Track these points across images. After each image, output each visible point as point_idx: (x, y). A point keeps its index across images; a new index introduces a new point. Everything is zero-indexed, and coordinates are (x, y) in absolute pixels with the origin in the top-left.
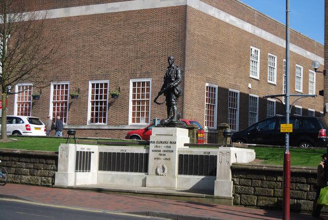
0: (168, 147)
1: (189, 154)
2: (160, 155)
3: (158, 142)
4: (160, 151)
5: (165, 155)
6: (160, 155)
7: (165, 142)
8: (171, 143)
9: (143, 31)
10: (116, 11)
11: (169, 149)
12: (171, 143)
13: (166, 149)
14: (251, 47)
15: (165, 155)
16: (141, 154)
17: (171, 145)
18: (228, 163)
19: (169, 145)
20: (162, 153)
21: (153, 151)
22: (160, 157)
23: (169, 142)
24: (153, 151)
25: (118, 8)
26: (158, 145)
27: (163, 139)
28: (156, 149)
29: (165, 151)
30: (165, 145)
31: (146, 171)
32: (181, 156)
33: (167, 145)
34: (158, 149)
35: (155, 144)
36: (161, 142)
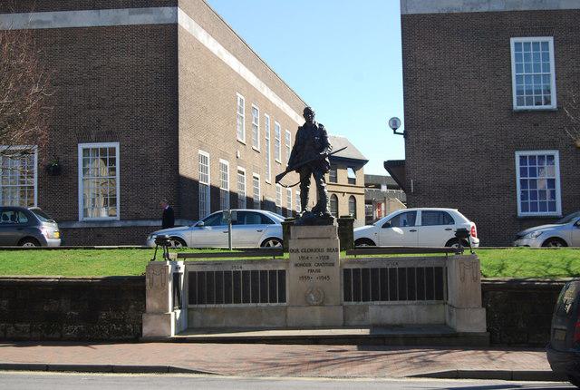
1: (361, 267)
2: (312, 271)
3: (304, 251)
5: (319, 271)
6: (312, 271)
8: (329, 250)
9: (98, 63)
10: (46, 27)
12: (329, 250)
14: (238, 94)
16: (273, 273)
17: (328, 254)
18: (476, 279)
20: (315, 268)
21: (296, 265)
22: (310, 274)
24: (296, 265)
25: (49, 22)
26: (304, 254)
27: (314, 244)
28: (300, 262)
30: (316, 254)
31: (283, 299)
32: (346, 272)
33: (321, 254)
34: (307, 261)
36: (311, 250)
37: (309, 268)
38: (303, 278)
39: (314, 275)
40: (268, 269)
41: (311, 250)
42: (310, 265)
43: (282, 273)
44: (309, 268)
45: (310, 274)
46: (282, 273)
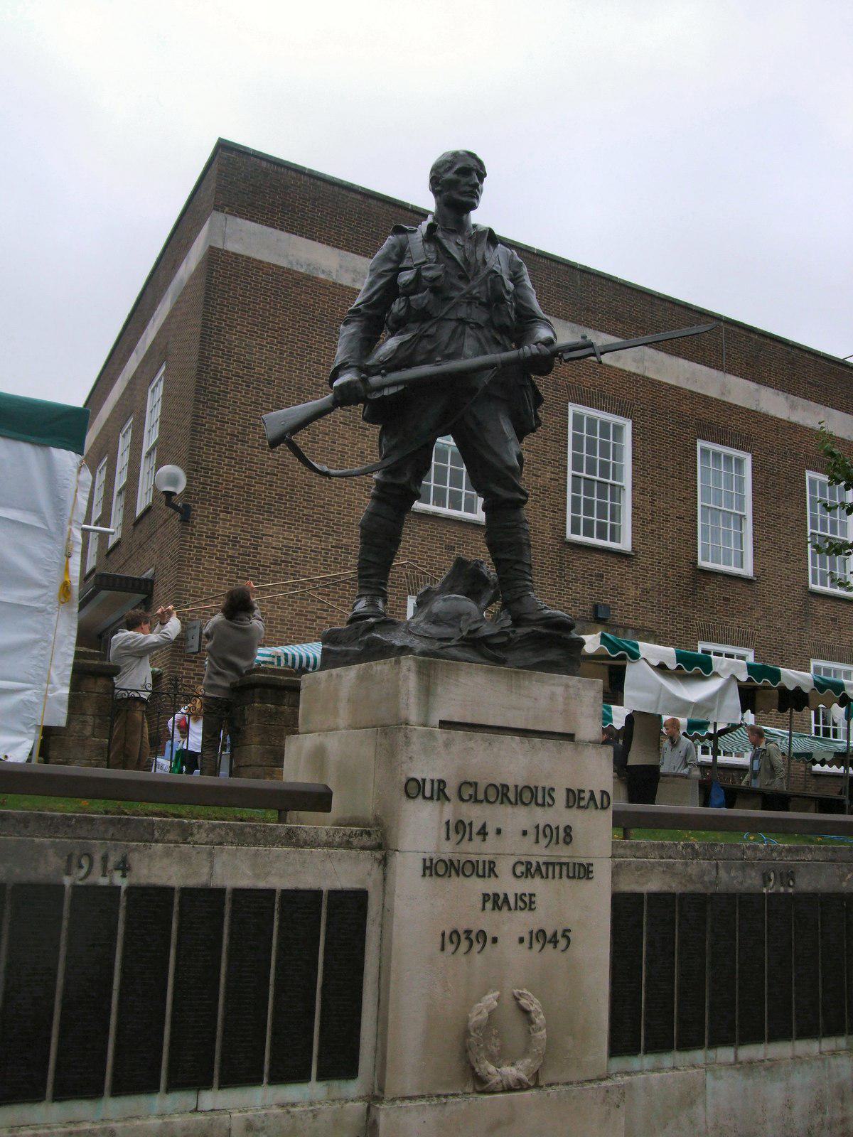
0: (548, 833)
2: (497, 902)
3: (471, 792)
4: (490, 870)
5: (527, 903)
6: (497, 902)
7: (530, 795)
11: (562, 853)
12: (575, 798)
13: (540, 853)
15: (527, 903)
16: (302, 903)
19: (558, 815)
20: (507, 885)
21: (430, 868)
23: (560, 796)
24: (430, 868)
26: (475, 814)
27: (513, 763)
28: (448, 850)
29: (528, 873)
32: (626, 909)
33: (542, 816)
34: (475, 849)
35: (449, 811)
36: (501, 794)
37: (490, 886)
38: (463, 939)
39: (513, 925)
40: (278, 881)
41: (501, 794)
42: (490, 870)
43: (351, 907)
44: (490, 886)
45: (487, 921)
46: (351, 907)
